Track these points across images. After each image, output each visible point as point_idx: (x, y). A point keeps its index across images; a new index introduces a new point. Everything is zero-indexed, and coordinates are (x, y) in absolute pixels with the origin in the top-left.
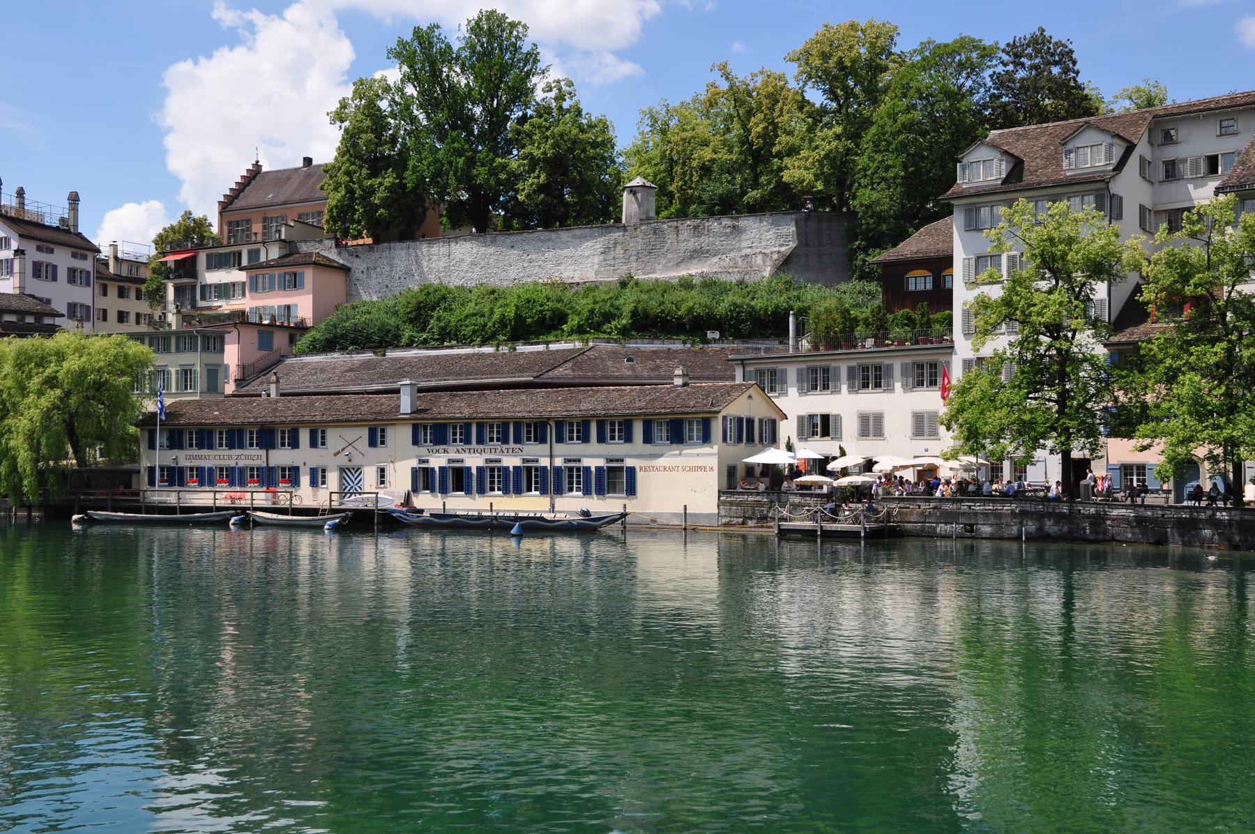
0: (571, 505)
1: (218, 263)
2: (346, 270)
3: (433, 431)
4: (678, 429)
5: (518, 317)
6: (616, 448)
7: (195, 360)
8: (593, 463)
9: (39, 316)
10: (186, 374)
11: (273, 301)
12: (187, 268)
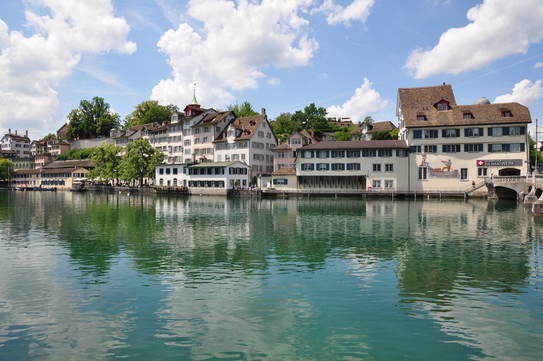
0: (50, 187)
1: (50, 143)
2: (69, 145)
3: (44, 175)
4: (68, 175)
5: (82, 155)
6: (62, 178)
7: (28, 162)
8: (60, 180)
9: (13, 154)
10: (27, 165)
11: (55, 151)
12: (45, 144)
